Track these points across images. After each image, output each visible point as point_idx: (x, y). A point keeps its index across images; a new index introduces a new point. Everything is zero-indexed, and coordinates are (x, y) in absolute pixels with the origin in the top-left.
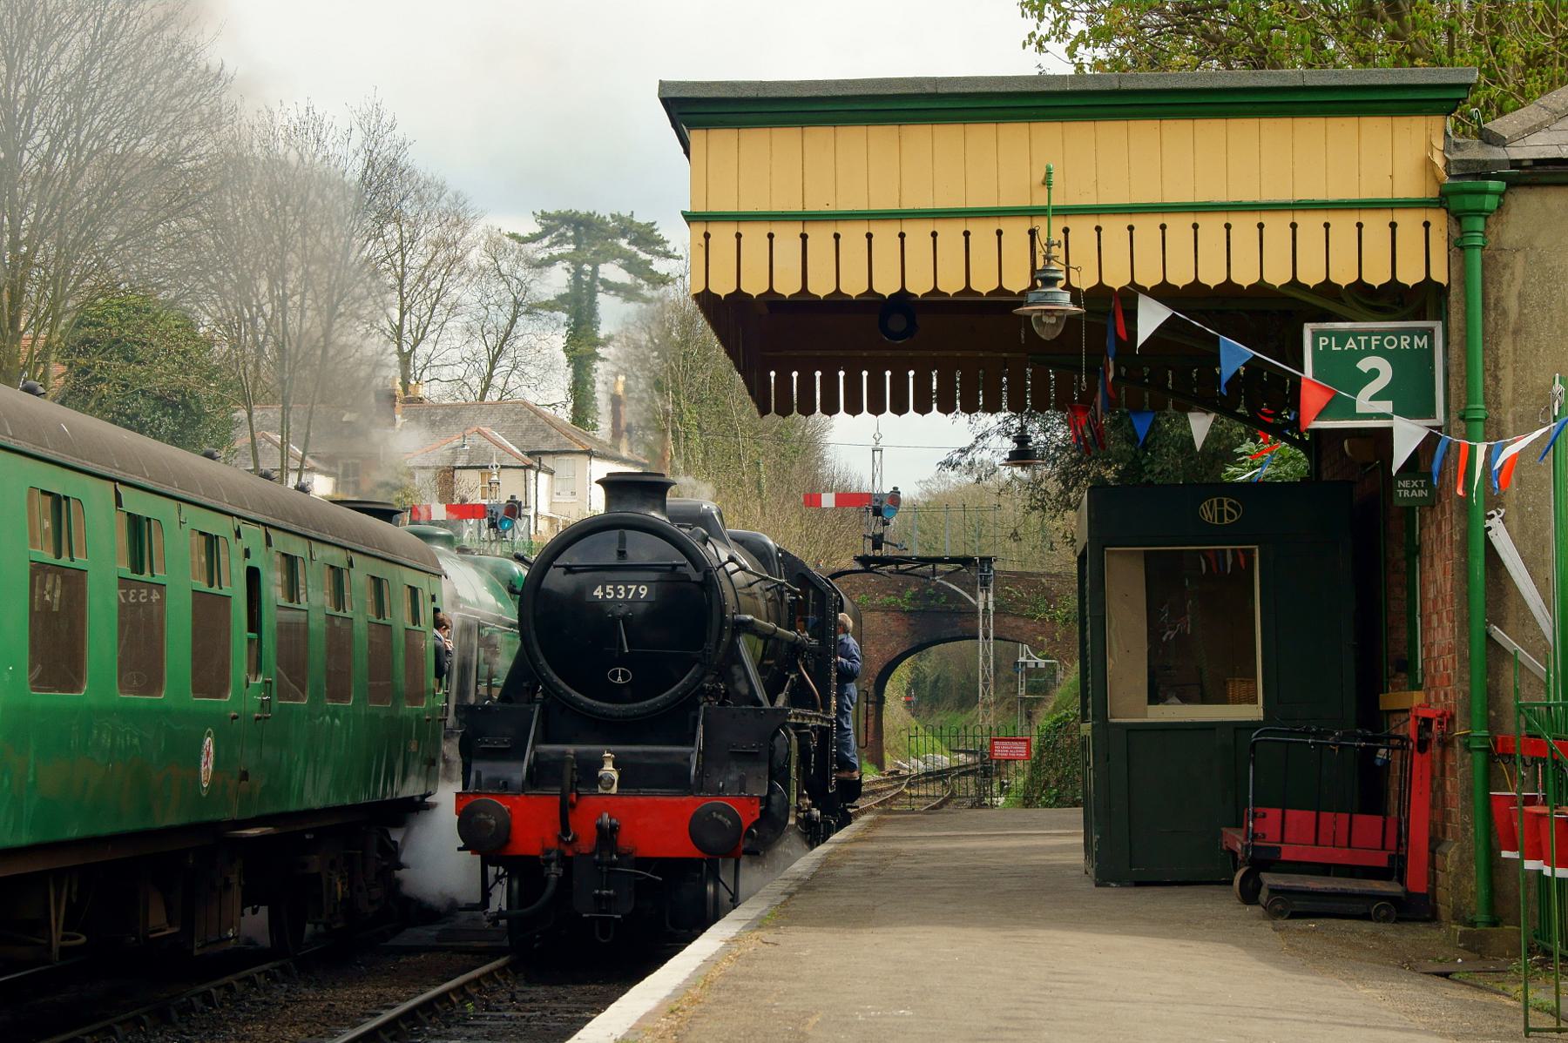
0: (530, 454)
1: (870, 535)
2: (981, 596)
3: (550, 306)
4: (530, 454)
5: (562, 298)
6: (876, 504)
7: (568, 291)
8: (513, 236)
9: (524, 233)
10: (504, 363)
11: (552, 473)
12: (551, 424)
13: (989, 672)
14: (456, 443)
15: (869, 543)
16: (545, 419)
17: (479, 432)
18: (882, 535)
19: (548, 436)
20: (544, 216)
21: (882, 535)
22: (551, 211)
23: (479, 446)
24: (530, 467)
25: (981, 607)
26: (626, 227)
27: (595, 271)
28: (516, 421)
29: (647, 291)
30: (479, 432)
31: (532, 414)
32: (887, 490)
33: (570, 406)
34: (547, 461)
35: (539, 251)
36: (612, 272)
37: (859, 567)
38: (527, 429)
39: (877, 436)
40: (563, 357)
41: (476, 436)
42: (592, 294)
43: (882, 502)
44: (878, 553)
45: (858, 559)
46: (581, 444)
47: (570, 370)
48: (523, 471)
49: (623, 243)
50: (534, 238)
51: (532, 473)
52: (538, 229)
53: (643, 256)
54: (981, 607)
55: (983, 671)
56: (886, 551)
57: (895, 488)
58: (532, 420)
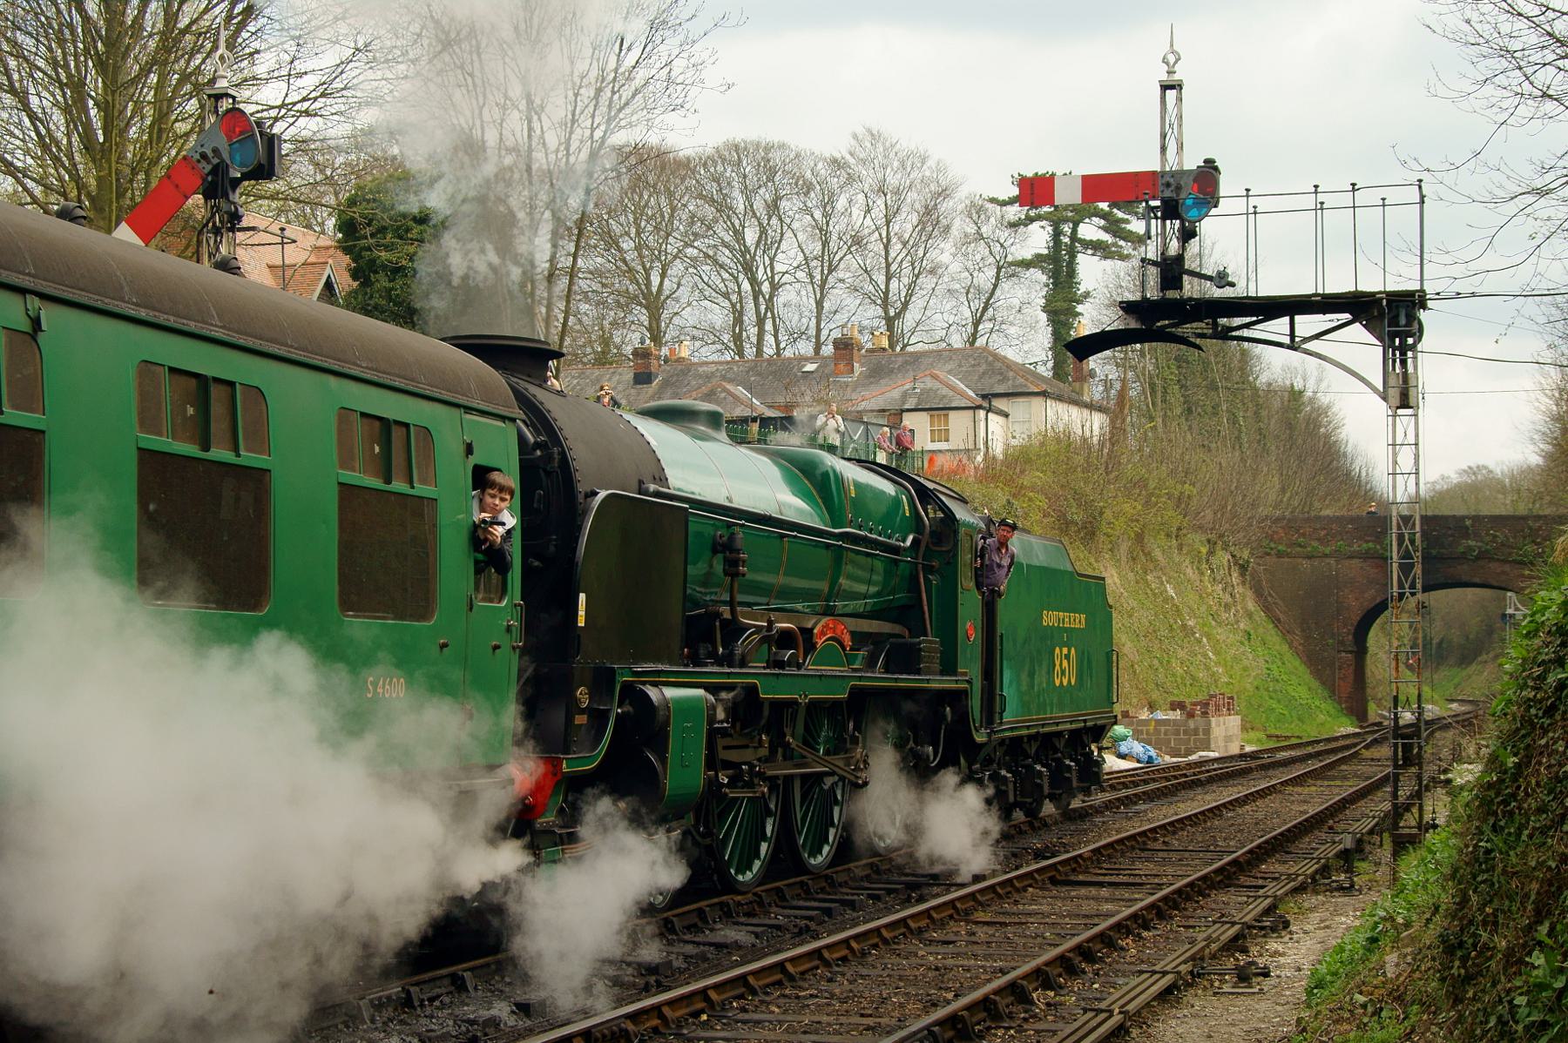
0: (984, 397)
3: (1026, 264)
4: (984, 397)
5: (1039, 257)
6: (1168, 194)
7: (1046, 252)
8: (993, 200)
9: (1003, 197)
10: (985, 326)
11: (1006, 415)
12: (1008, 367)
13: (1412, 542)
14: (907, 387)
15: (1153, 273)
16: (1003, 363)
17: (935, 377)
19: (1005, 379)
21: (1180, 258)
23: (931, 389)
24: (980, 407)
27: (1074, 231)
28: (974, 366)
29: (1127, 247)
30: (935, 377)
31: (991, 358)
32: (1192, 162)
33: (1050, 364)
34: (999, 404)
35: (1015, 212)
36: (1090, 230)
38: (983, 373)
39: (1172, 59)
40: (1043, 317)
41: (928, 379)
42: (1073, 255)
43: (1179, 188)
44: (1172, 294)
45: (1128, 308)
46: (1037, 386)
47: (1050, 329)
48: (970, 412)
50: (1011, 202)
51: (982, 413)
53: (1120, 215)
55: (1401, 538)
57: (1210, 163)
58: (990, 364)
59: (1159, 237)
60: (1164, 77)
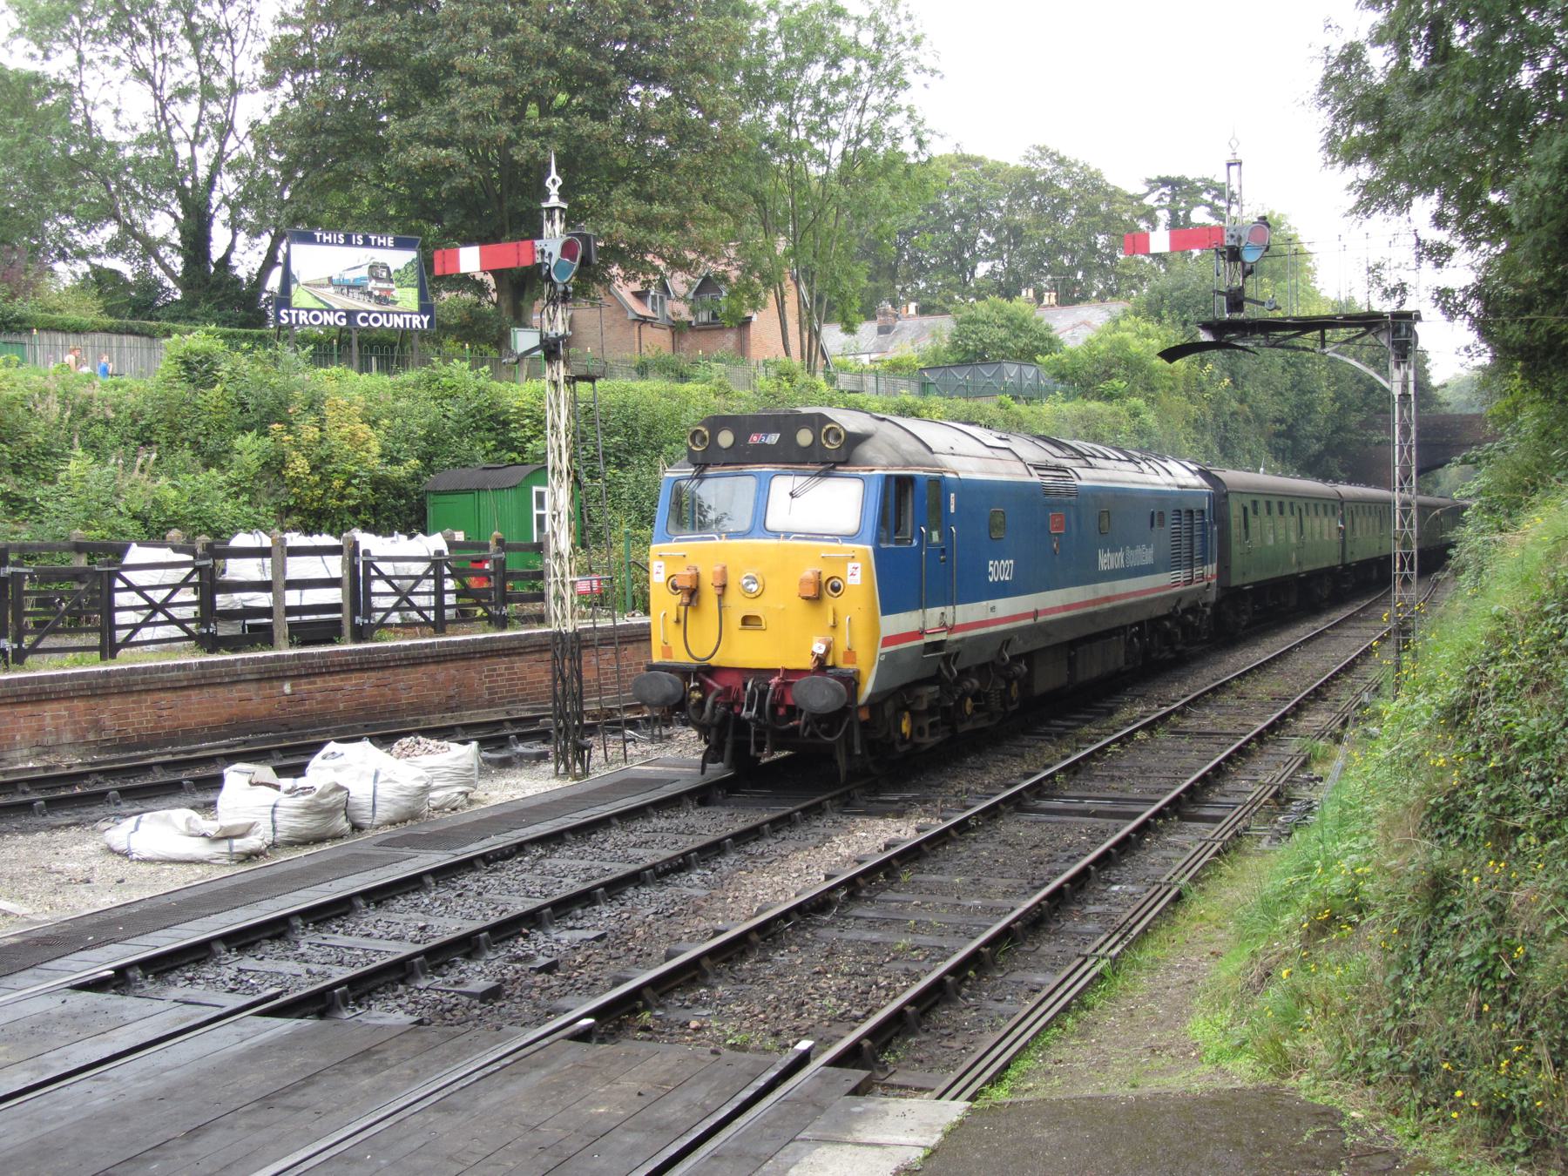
1: (1223, 289)
2: (1397, 375)
6: (1231, 243)
18: (1241, 290)
20: (1149, 181)
21: (1241, 290)
22: (1154, 177)
25: (1397, 391)
26: (1209, 185)
37: (1205, 337)
39: (1234, 143)
43: (1240, 239)
44: (1237, 316)
49: (1206, 197)
52: (1146, 189)
54: (1397, 391)
56: (1250, 312)
59: (1228, 277)
60: (1231, 158)
